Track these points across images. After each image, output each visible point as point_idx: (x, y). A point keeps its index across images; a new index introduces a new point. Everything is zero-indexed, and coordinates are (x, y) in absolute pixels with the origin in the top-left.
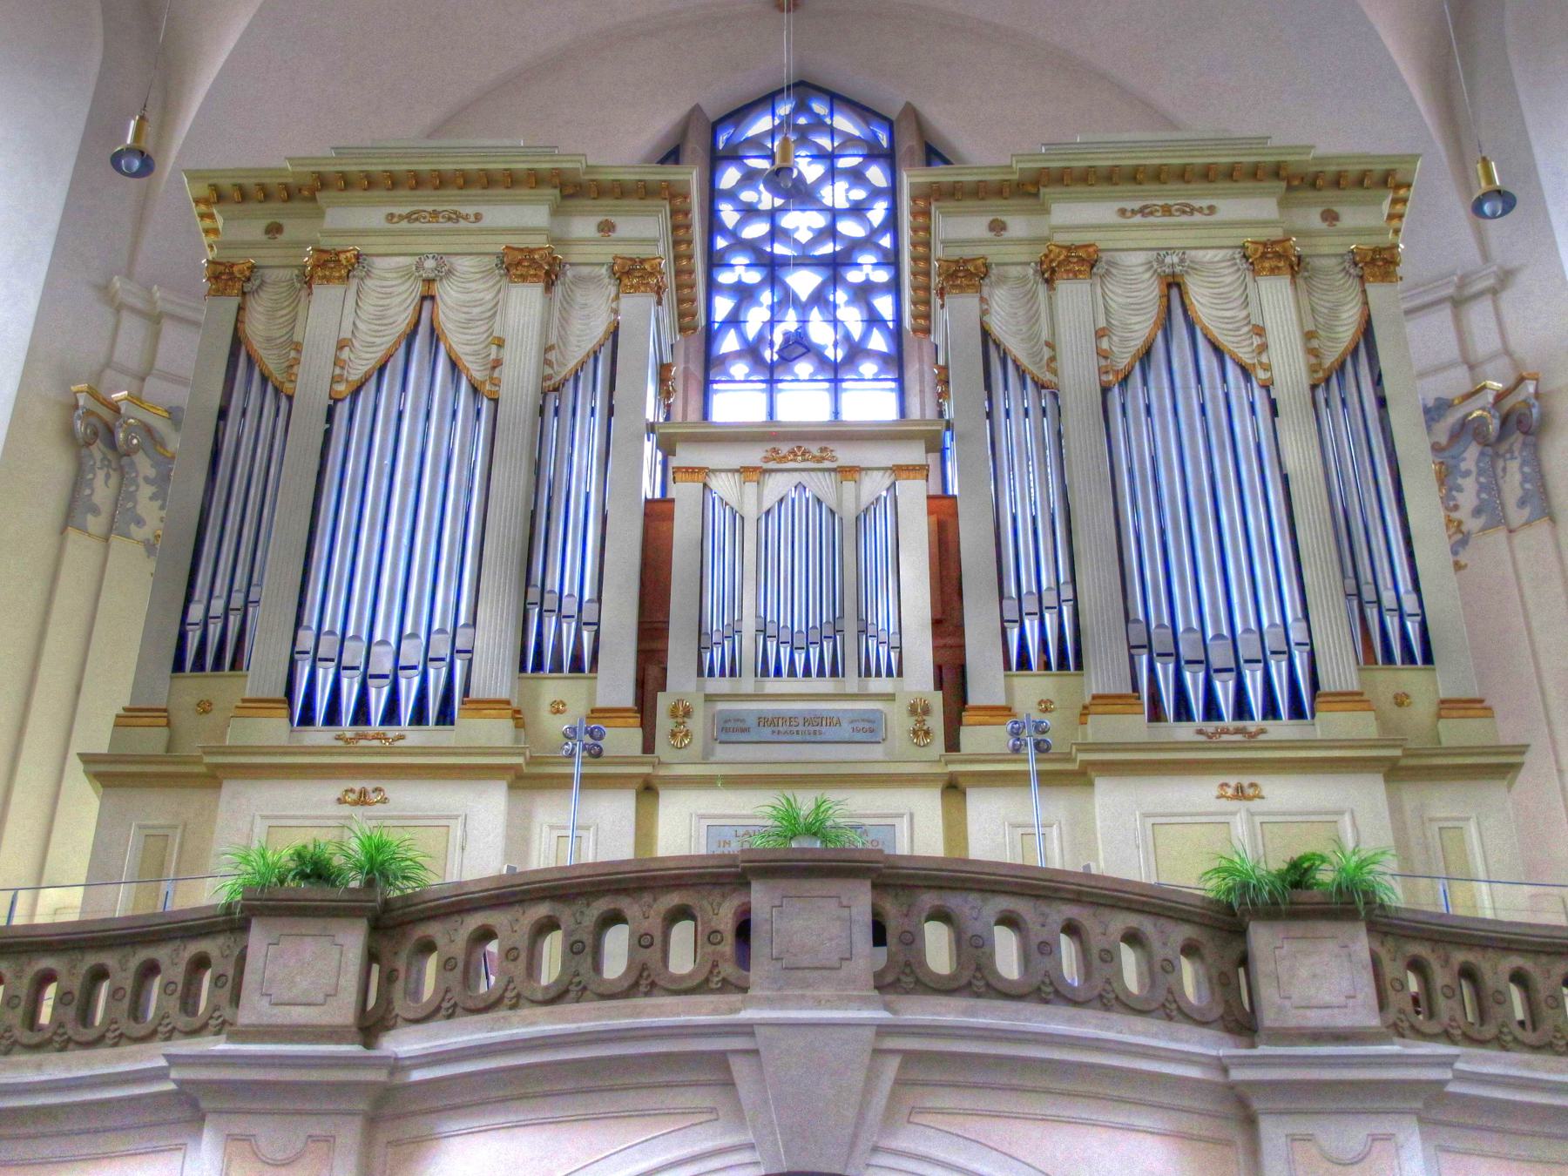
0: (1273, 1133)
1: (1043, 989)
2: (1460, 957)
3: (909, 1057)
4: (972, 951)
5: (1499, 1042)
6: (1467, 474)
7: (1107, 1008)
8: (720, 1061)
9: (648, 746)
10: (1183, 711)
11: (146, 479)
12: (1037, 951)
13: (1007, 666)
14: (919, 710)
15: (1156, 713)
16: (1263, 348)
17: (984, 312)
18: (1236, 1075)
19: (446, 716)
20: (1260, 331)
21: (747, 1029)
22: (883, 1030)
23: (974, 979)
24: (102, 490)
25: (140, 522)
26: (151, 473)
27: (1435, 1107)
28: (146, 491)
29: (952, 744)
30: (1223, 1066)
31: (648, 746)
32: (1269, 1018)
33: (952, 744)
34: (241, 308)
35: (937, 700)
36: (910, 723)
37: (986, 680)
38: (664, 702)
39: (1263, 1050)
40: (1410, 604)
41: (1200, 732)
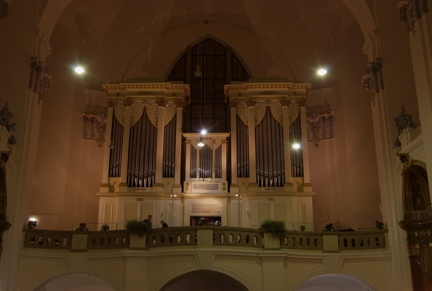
0: (264, 263)
1: (234, 244)
2: (293, 236)
3: (217, 255)
4: (226, 239)
5: (297, 248)
6: (321, 128)
7: (244, 246)
8: (193, 255)
9: (183, 192)
10: (264, 186)
11: (96, 128)
12: (234, 239)
13: (238, 177)
14: (224, 184)
15: (260, 186)
16: (282, 120)
17: (237, 111)
18: (260, 255)
19: (151, 186)
20: (282, 117)
21: (197, 252)
22: (214, 252)
23: (227, 243)
24: (89, 131)
25: (95, 136)
26: (96, 126)
27: (286, 259)
28: (95, 130)
29: (229, 191)
30: (258, 254)
31: (183, 192)
32: (265, 247)
33: (229, 191)
34: (114, 110)
35: (226, 183)
36: (223, 187)
37: (234, 179)
38: (185, 183)
39: (265, 252)
40: (301, 167)
41: (266, 189)
